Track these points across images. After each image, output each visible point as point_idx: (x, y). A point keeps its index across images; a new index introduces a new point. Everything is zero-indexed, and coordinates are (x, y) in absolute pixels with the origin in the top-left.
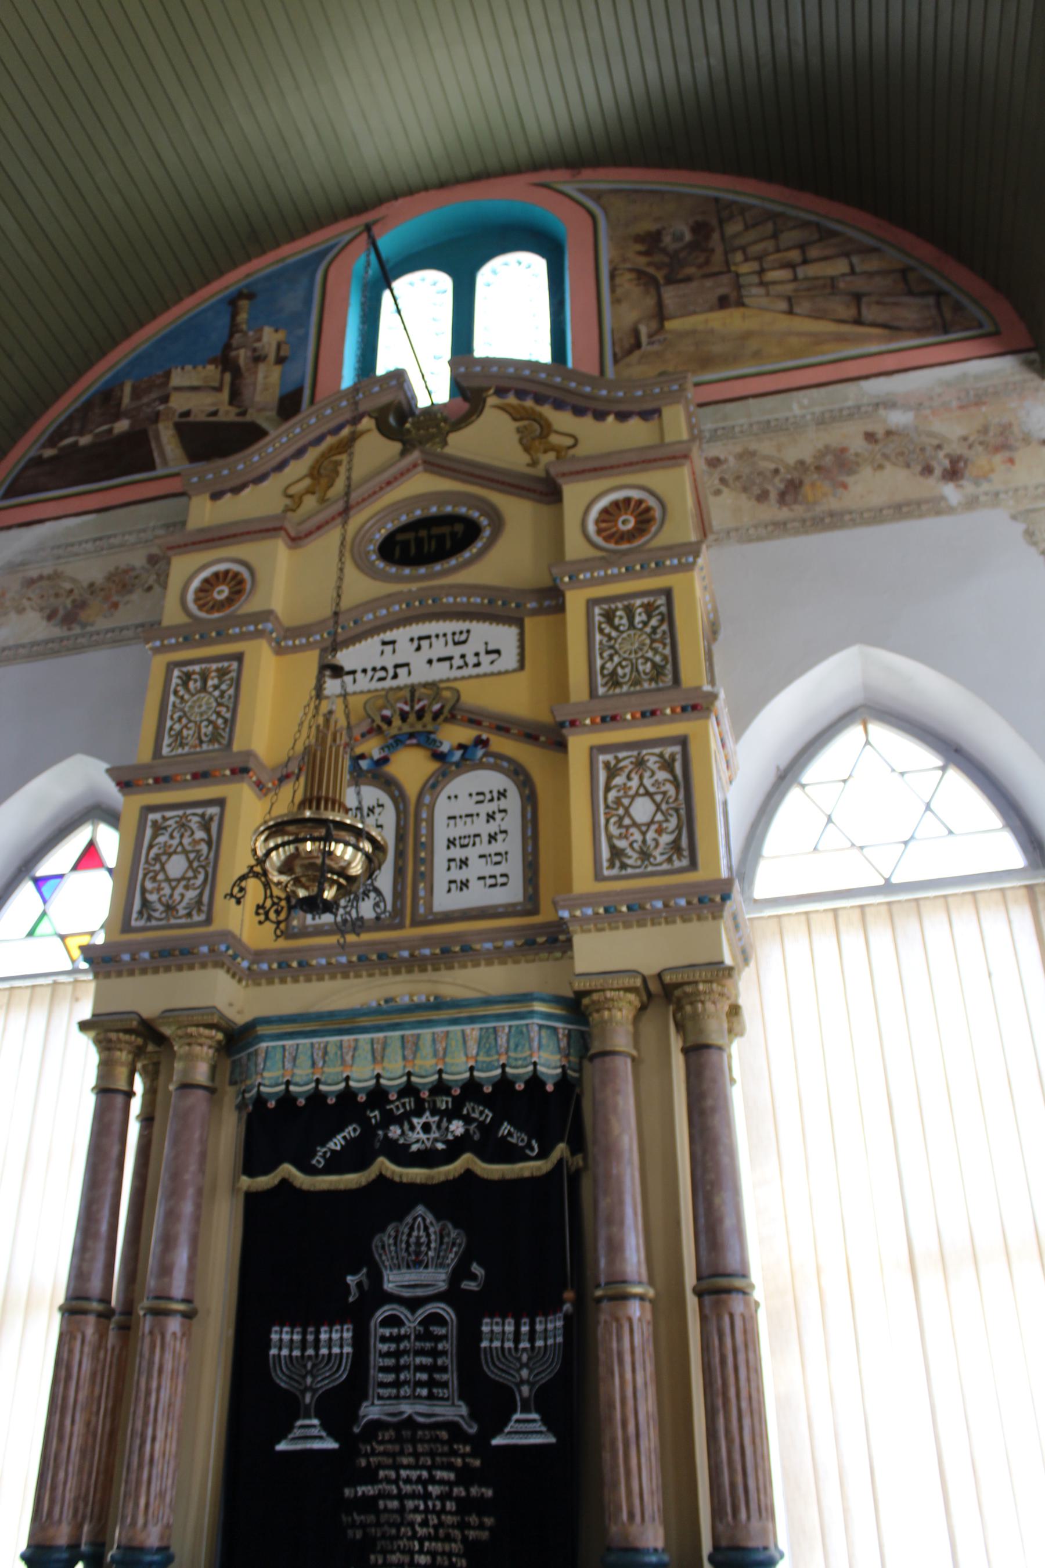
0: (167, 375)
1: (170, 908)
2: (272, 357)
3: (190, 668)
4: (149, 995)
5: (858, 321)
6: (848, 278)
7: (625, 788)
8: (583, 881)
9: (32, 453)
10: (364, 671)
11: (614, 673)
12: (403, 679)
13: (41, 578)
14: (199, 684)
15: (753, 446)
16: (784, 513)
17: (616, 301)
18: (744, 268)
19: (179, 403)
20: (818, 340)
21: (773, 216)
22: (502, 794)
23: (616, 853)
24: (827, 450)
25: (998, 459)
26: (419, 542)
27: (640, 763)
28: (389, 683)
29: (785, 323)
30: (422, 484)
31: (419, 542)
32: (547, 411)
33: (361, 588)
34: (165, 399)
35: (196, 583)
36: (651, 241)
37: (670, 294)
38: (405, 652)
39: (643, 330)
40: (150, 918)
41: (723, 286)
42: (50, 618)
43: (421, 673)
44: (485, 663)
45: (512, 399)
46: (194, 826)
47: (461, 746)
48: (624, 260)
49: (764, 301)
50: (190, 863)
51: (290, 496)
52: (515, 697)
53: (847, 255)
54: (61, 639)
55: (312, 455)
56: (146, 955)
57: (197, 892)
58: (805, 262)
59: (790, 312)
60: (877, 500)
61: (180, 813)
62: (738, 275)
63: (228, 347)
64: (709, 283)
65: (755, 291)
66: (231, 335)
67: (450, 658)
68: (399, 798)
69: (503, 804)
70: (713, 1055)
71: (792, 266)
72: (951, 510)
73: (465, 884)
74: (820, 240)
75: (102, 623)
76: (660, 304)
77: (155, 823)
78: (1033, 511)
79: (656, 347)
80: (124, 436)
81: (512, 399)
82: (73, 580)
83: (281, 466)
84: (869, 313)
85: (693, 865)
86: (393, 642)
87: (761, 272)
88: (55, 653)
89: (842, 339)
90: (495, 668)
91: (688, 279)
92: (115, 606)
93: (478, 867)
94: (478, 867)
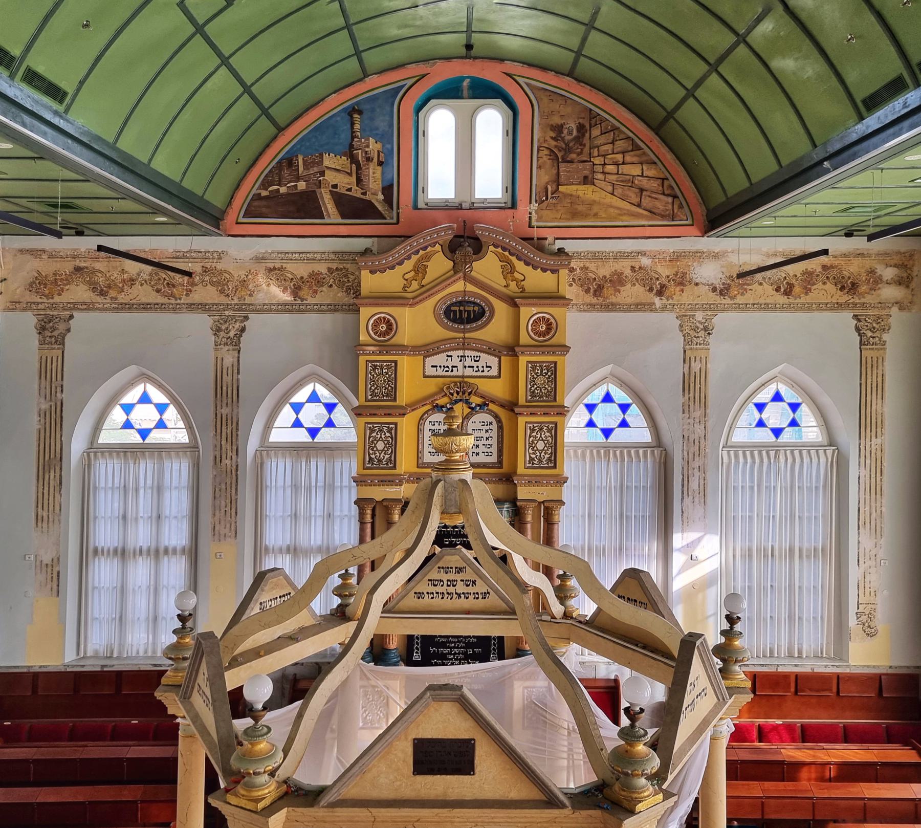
0: (321, 156)
2: (376, 160)
4: (379, 493)
5: (639, 206)
6: (640, 178)
7: (536, 437)
8: (521, 470)
9: (254, 191)
11: (534, 391)
12: (455, 373)
13: (275, 269)
15: (588, 265)
17: (539, 167)
18: (597, 161)
20: (623, 213)
21: (615, 129)
22: (491, 423)
23: (531, 459)
24: (615, 273)
26: (460, 311)
27: (541, 429)
28: (449, 373)
29: (610, 199)
31: (460, 311)
33: (438, 331)
34: (322, 173)
37: (563, 167)
38: (456, 361)
39: (549, 187)
41: (585, 170)
44: (487, 373)
45: (499, 250)
47: (479, 405)
48: (545, 141)
49: (603, 184)
52: (497, 389)
53: (642, 164)
54: (292, 305)
55: (414, 258)
58: (623, 163)
59: (612, 194)
62: (594, 165)
63: (351, 146)
64: (581, 166)
66: (352, 140)
69: (491, 427)
70: (556, 526)
71: (617, 164)
73: (478, 454)
74: (632, 151)
75: (310, 300)
76: (558, 174)
79: (554, 201)
81: (499, 250)
82: (292, 274)
84: (646, 202)
85: (555, 467)
87: (605, 164)
90: (489, 374)
91: (571, 162)
92: (316, 292)
93: (482, 449)
94: (482, 449)
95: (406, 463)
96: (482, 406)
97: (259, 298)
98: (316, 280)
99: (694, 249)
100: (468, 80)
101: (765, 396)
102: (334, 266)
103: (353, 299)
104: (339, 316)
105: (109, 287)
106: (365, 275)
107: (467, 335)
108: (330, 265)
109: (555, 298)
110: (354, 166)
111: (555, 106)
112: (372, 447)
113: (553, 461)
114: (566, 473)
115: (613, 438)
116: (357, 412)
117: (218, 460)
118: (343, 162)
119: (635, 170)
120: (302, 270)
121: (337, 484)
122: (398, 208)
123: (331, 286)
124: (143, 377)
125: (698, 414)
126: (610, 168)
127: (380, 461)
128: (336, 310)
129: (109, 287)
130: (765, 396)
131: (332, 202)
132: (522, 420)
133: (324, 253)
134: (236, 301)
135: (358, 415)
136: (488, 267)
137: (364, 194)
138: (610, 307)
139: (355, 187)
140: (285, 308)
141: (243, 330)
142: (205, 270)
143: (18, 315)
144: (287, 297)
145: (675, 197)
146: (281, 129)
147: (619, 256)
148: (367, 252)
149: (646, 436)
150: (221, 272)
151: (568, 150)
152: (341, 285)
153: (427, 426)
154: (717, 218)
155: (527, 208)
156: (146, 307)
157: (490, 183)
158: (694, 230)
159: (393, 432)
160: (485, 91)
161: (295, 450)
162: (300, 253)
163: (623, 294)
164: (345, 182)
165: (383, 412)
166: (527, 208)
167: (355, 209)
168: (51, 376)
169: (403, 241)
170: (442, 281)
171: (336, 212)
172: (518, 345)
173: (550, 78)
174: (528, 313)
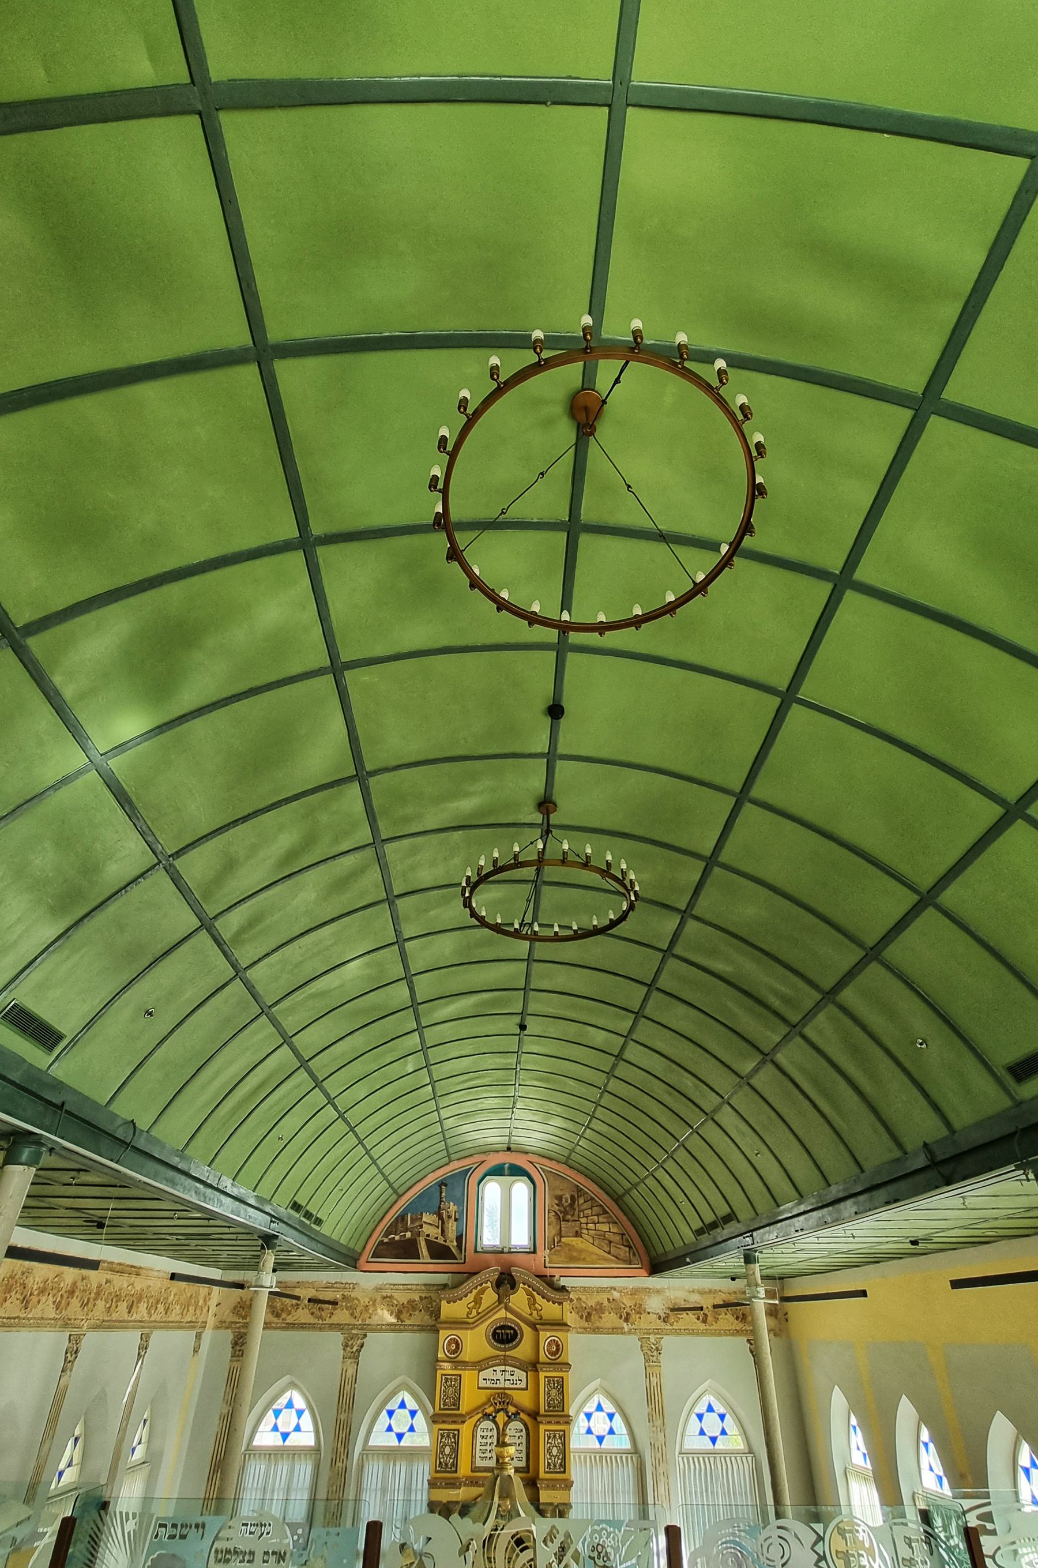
1: (446, 1465)
5: (609, 1253)
8: (542, 1475)
12: (498, 1386)
16: (586, 1325)
18: (584, 1220)
19: (427, 1230)
21: (592, 1199)
23: (549, 1464)
30: (502, 1313)
32: (535, 1293)
36: (559, 1198)
37: (563, 1224)
38: (499, 1376)
43: (501, 1384)
52: (524, 1399)
55: (475, 1292)
60: (609, 1325)
64: (574, 1223)
65: (585, 1231)
66: (441, 1201)
68: (498, 1428)
75: (407, 1322)
80: (409, 1239)
83: (466, 1296)
85: (564, 1472)
88: (393, 1331)
89: (606, 1260)
91: (568, 1221)
95: (464, 1469)
96: (516, 1414)
97: (375, 1320)
98: (412, 1305)
99: (645, 1286)
101: (701, 1408)
103: (434, 1324)
104: (424, 1334)
105: (282, 1310)
106: (444, 1303)
107: (508, 1353)
109: (560, 1324)
111: (557, 1183)
112: (443, 1447)
113: (564, 1467)
114: (573, 1478)
115: (605, 1445)
116: (434, 1419)
117: (333, 1463)
119: (605, 1228)
120: (402, 1298)
121: (413, 1487)
124: (292, 1385)
125: (659, 1422)
126: (591, 1226)
128: (422, 1330)
129: (282, 1310)
130: (701, 1408)
132: (542, 1428)
135: (434, 1422)
136: (519, 1299)
138: (596, 1330)
140: (392, 1328)
141: (362, 1346)
142: (344, 1297)
143: (222, 1331)
144: (393, 1320)
145: (630, 1247)
146: (400, 1196)
147: (600, 1290)
148: (445, 1286)
149: (627, 1445)
150: (354, 1299)
151: (565, 1213)
152: (427, 1309)
153: (479, 1433)
154: (657, 1267)
155: (543, 1253)
156: (303, 1326)
157: (520, 1238)
158: (643, 1272)
160: (517, 1171)
161: (389, 1454)
163: (604, 1320)
164: (434, 1232)
165: (450, 1419)
166: (543, 1253)
167: (440, 1252)
168: (234, 1382)
169: (468, 1279)
170: (491, 1310)
172: (538, 1362)
173: (553, 1164)
174: (546, 1336)
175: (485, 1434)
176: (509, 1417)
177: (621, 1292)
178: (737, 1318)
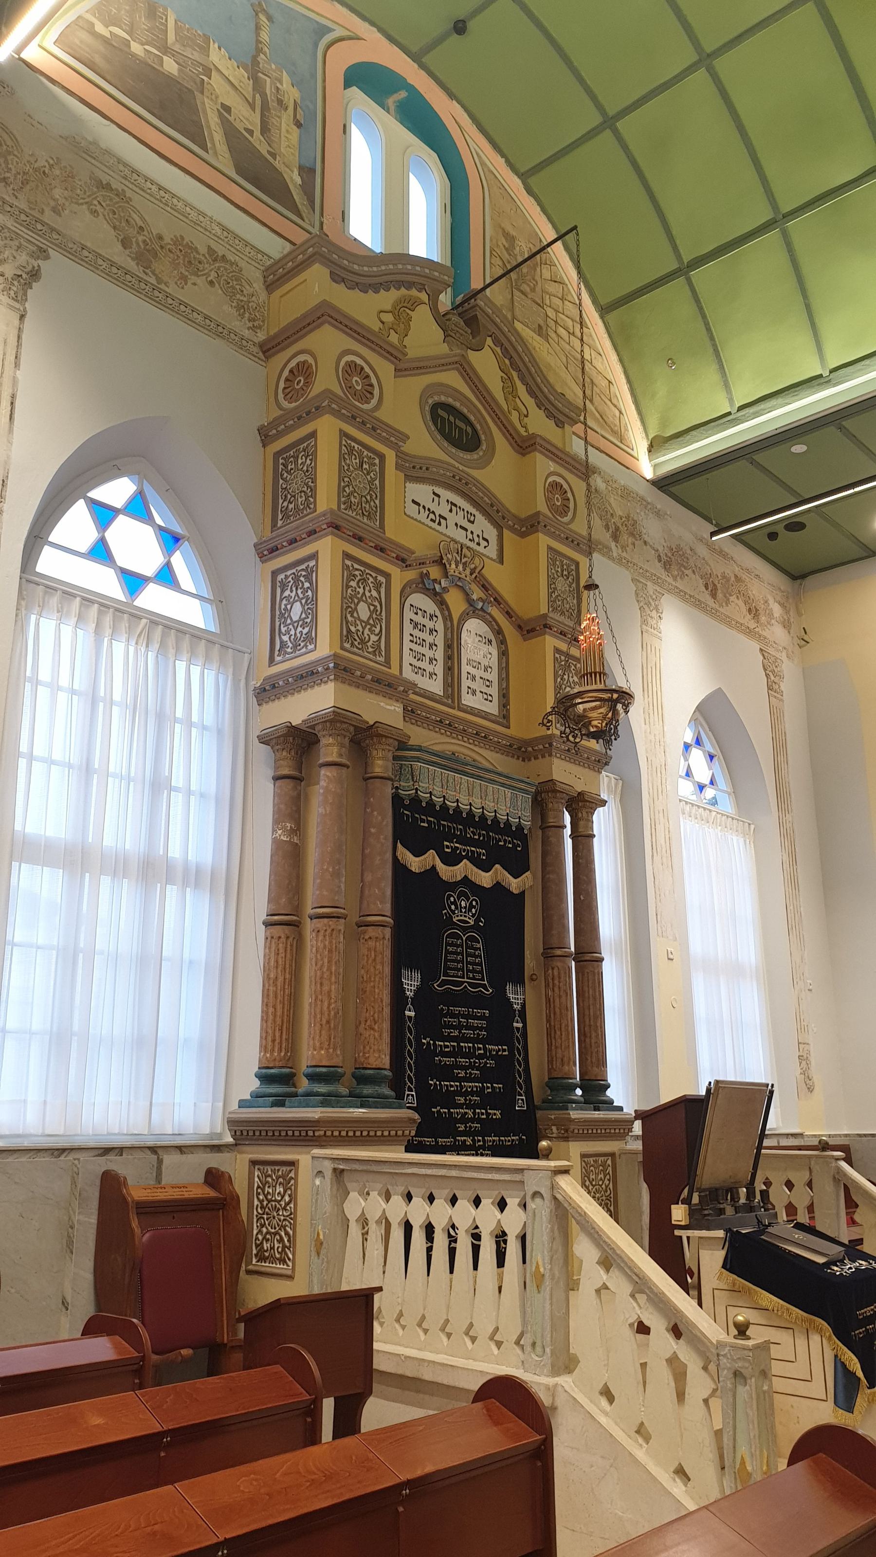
3: (353, 444)
10: (424, 507)
12: (442, 529)
13: (108, 187)
14: (357, 461)
25: (631, 540)
32: (515, 374)
34: (208, 72)
35: (342, 363)
40: (352, 645)
42: (125, 243)
46: (371, 585)
50: (371, 613)
51: (383, 323)
56: (369, 677)
57: (377, 638)
61: (362, 569)
65: (553, 335)
67: (466, 530)
68: (448, 617)
72: (612, 559)
77: (348, 566)
78: (639, 581)
83: (376, 288)
86: (439, 496)
92: (184, 279)
100: (403, 94)
102: (220, 251)
108: (214, 245)
110: (258, 96)
118: (239, 76)
122: (322, 215)
123: (211, 283)
127: (363, 642)
128: (220, 335)
131: (221, 131)
133: (204, 215)
134: (23, 205)
137: (274, 155)
139: (257, 133)
141: (35, 275)
159: (383, 590)
162: (161, 188)
171: (228, 155)
175: (418, 619)
176: (470, 602)
177: (607, 482)
178: (750, 610)
